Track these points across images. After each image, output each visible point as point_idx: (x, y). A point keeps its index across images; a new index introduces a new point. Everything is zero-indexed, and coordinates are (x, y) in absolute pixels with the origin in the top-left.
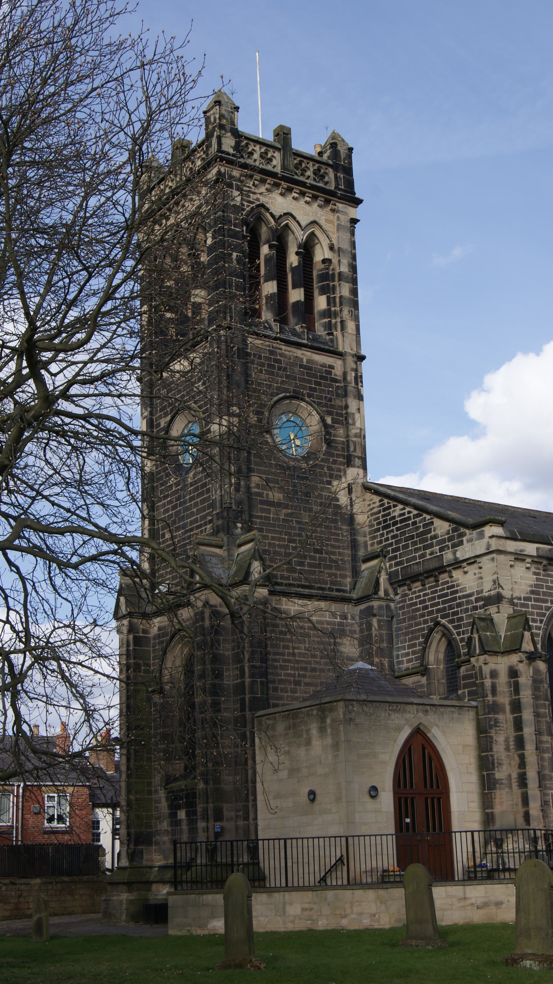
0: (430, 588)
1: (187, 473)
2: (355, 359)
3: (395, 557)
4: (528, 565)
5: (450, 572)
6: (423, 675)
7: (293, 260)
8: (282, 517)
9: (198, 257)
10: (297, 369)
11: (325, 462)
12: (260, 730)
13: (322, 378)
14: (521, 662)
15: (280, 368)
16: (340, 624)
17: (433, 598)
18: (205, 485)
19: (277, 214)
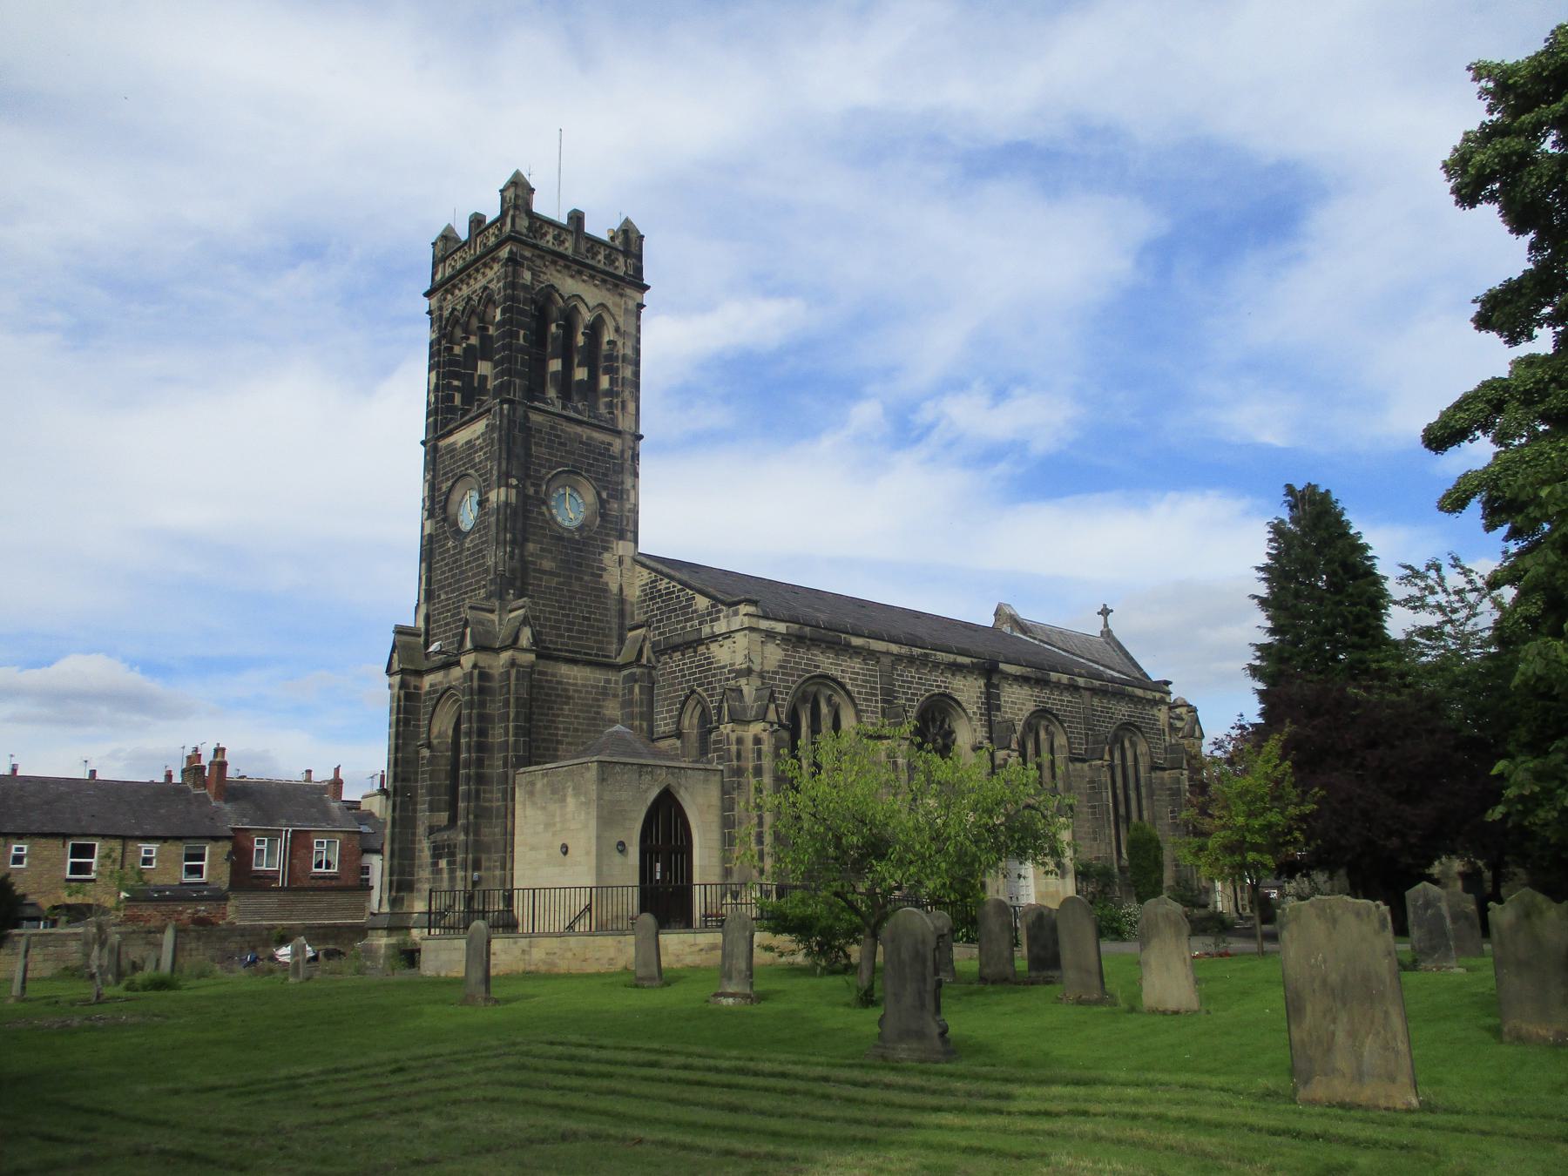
0: (689, 658)
1: (465, 538)
3: (659, 628)
5: (707, 644)
6: (678, 739)
7: (580, 340)
8: (554, 585)
9: (487, 329)
10: (576, 445)
12: (520, 786)
13: (600, 454)
14: (765, 730)
15: (561, 444)
16: (604, 688)
17: (691, 668)
18: (480, 551)
19: (566, 296)
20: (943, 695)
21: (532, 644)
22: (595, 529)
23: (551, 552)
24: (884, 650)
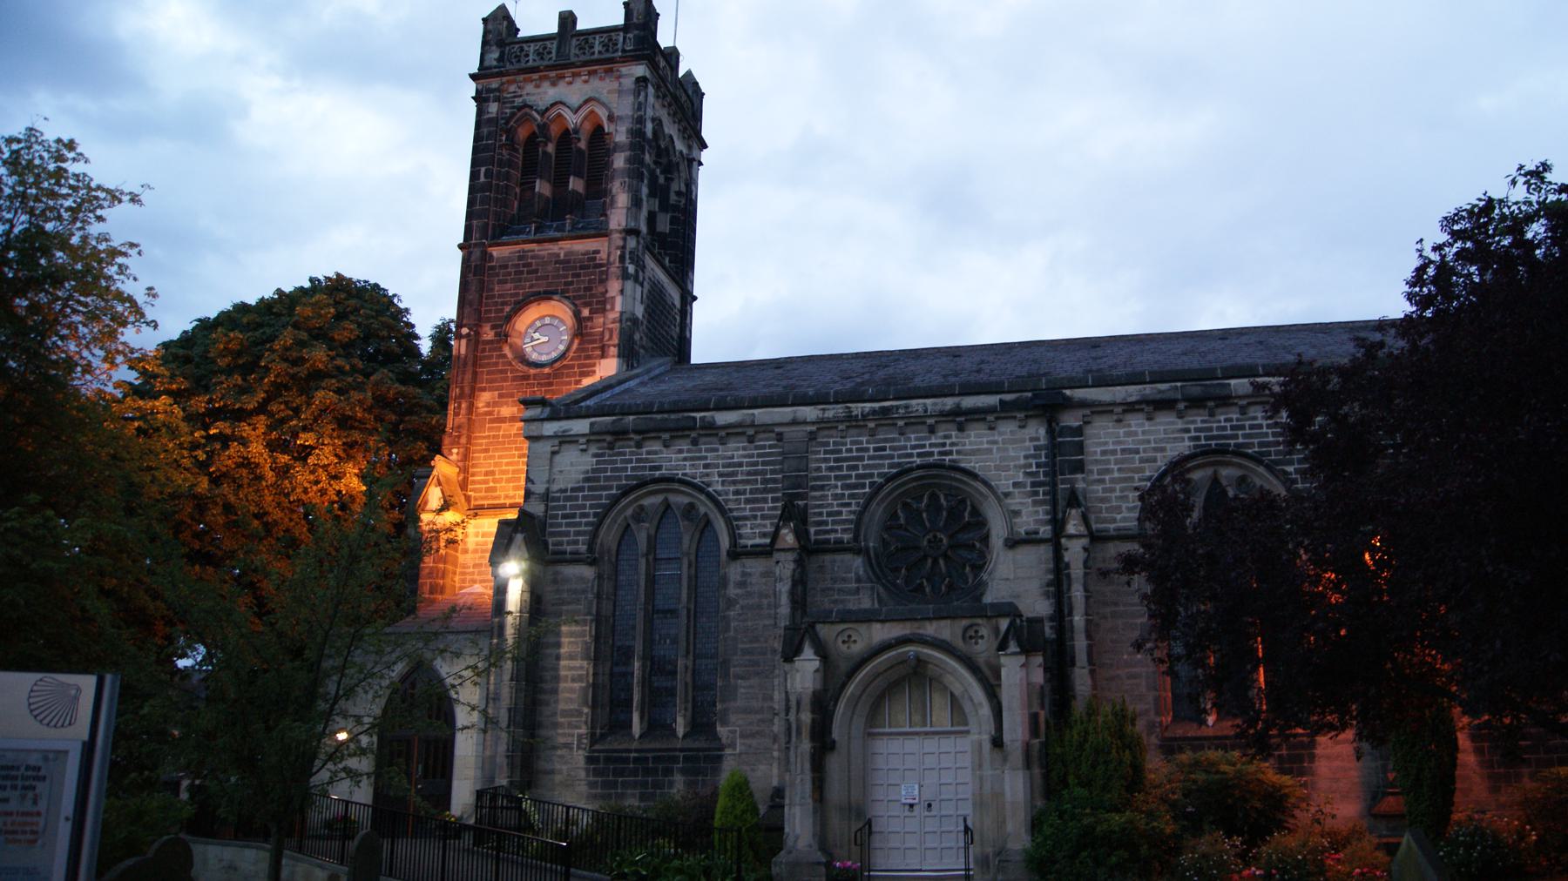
2: (623, 235)
4: (584, 447)
11: (576, 360)
13: (581, 268)
20: (939, 466)
22: (571, 354)
23: (512, 396)
24: (788, 418)
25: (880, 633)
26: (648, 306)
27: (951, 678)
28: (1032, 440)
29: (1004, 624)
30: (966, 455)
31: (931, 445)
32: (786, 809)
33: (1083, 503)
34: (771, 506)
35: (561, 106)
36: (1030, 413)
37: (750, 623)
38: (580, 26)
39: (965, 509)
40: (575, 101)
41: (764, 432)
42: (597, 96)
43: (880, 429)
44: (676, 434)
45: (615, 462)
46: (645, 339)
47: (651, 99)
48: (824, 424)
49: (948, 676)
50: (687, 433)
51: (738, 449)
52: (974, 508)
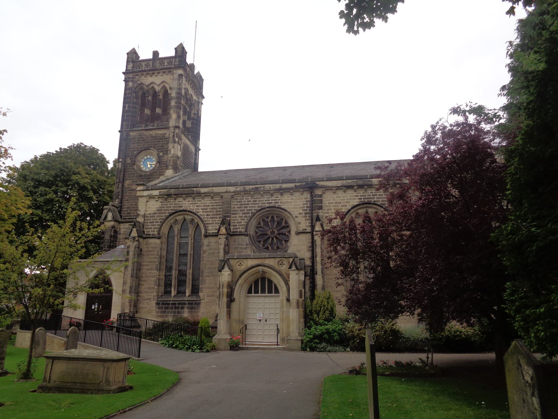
2: (174, 128)
4: (157, 199)
13: (160, 139)
21: (113, 218)
22: (156, 168)
24: (224, 191)
25: (251, 263)
26: (183, 152)
27: (274, 277)
28: (305, 198)
29: (291, 260)
30: (283, 203)
31: (272, 200)
32: (218, 321)
33: (321, 220)
34: (218, 220)
35: (154, 84)
36: (305, 190)
37: (210, 259)
38: (160, 56)
39: (283, 221)
40: (158, 82)
41: (217, 195)
42: (166, 80)
43: (255, 194)
44: (187, 195)
45: (167, 204)
46: (181, 163)
47: (184, 82)
48: (236, 193)
49: (273, 277)
50: (191, 195)
51: (208, 201)
52: (286, 221)
